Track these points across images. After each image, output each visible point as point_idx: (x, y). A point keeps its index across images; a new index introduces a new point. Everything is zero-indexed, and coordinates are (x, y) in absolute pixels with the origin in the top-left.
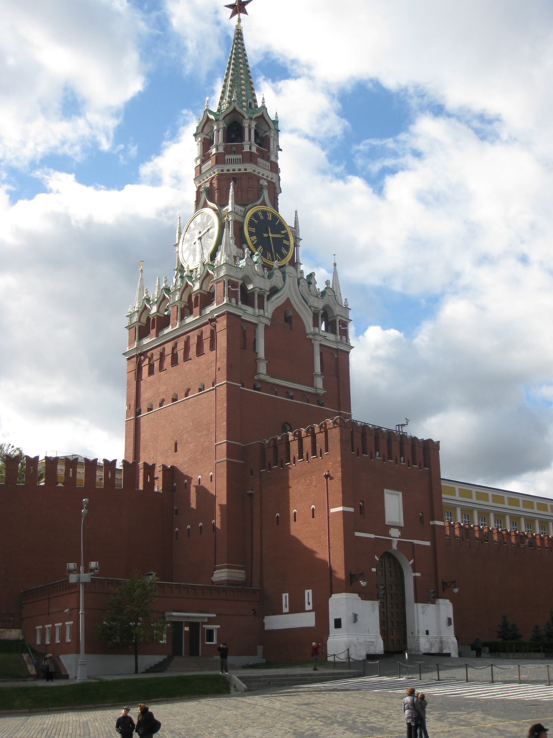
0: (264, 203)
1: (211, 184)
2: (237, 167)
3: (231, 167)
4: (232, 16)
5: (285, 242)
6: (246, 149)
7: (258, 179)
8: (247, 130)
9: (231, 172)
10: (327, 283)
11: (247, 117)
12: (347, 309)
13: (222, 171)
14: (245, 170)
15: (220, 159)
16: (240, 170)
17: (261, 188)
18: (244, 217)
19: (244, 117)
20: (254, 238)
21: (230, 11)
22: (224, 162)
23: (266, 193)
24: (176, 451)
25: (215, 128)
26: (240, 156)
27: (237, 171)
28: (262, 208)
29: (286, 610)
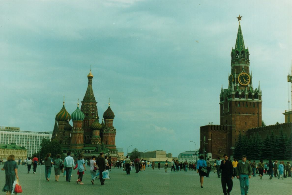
0: (243, 72)
2: (237, 65)
3: (236, 65)
5: (248, 79)
7: (242, 66)
9: (236, 66)
10: (256, 89)
12: (261, 93)
17: (243, 68)
18: (238, 77)
20: (240, 81)
21: (238, 19)
22: (235, 64)
23: (243, 70)
27: (237, 65)
28: (243, 73)
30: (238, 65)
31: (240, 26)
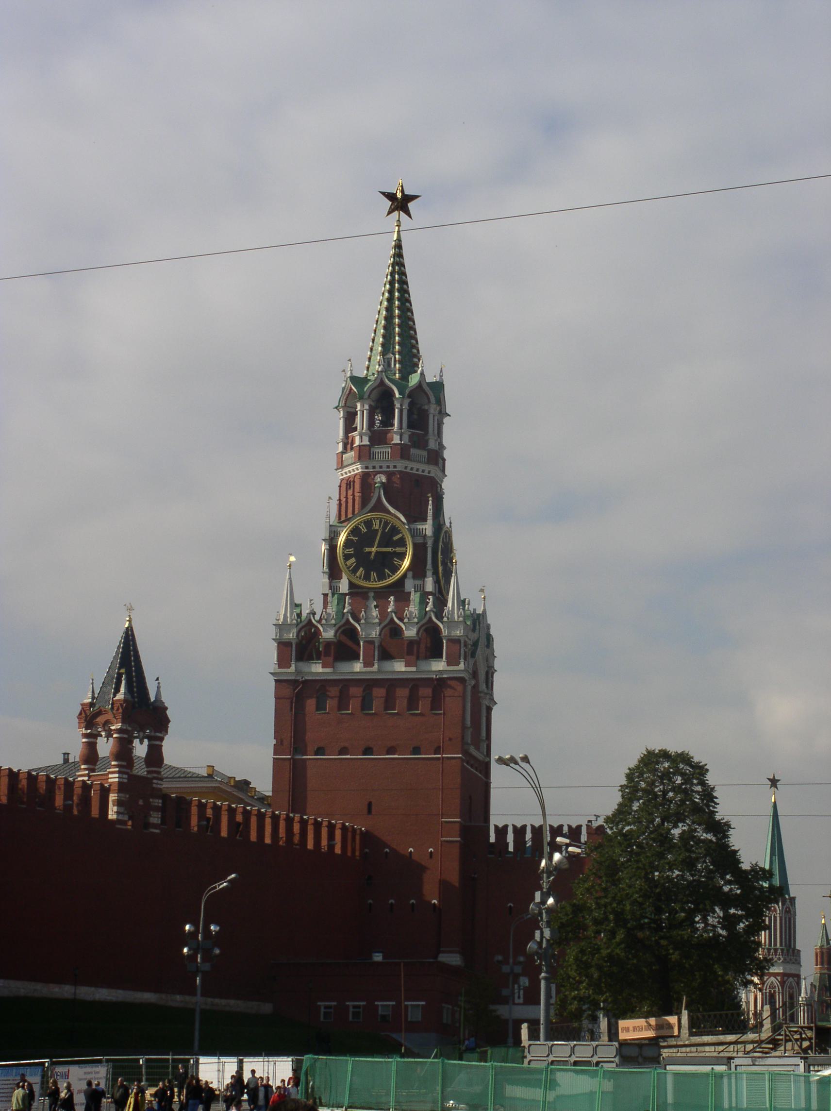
1: (388, 479)
2: (422, 467)
3: (415, 466)
4: (389, 213)
6: (432, 445)
8: (431, 417)
9: (414, 472)
11: (433, 399)
13: (406, 468)
14: (429, 472)
15: (403, 452)
16: (423, 471)
19: (429, 402)
24: (369, 811)
25: (398, 405)
26: (425, 453)
27: (420, 473)
29: (521, 1001)
30: (427, 468)
31: (398, 246)
